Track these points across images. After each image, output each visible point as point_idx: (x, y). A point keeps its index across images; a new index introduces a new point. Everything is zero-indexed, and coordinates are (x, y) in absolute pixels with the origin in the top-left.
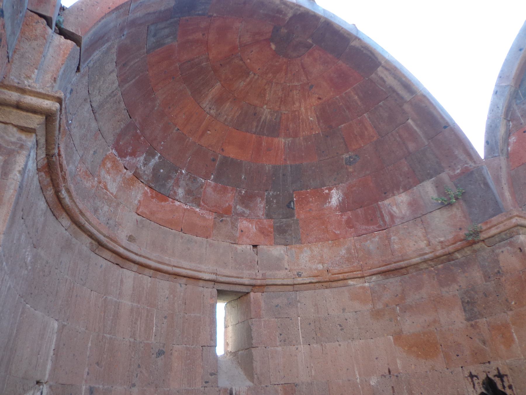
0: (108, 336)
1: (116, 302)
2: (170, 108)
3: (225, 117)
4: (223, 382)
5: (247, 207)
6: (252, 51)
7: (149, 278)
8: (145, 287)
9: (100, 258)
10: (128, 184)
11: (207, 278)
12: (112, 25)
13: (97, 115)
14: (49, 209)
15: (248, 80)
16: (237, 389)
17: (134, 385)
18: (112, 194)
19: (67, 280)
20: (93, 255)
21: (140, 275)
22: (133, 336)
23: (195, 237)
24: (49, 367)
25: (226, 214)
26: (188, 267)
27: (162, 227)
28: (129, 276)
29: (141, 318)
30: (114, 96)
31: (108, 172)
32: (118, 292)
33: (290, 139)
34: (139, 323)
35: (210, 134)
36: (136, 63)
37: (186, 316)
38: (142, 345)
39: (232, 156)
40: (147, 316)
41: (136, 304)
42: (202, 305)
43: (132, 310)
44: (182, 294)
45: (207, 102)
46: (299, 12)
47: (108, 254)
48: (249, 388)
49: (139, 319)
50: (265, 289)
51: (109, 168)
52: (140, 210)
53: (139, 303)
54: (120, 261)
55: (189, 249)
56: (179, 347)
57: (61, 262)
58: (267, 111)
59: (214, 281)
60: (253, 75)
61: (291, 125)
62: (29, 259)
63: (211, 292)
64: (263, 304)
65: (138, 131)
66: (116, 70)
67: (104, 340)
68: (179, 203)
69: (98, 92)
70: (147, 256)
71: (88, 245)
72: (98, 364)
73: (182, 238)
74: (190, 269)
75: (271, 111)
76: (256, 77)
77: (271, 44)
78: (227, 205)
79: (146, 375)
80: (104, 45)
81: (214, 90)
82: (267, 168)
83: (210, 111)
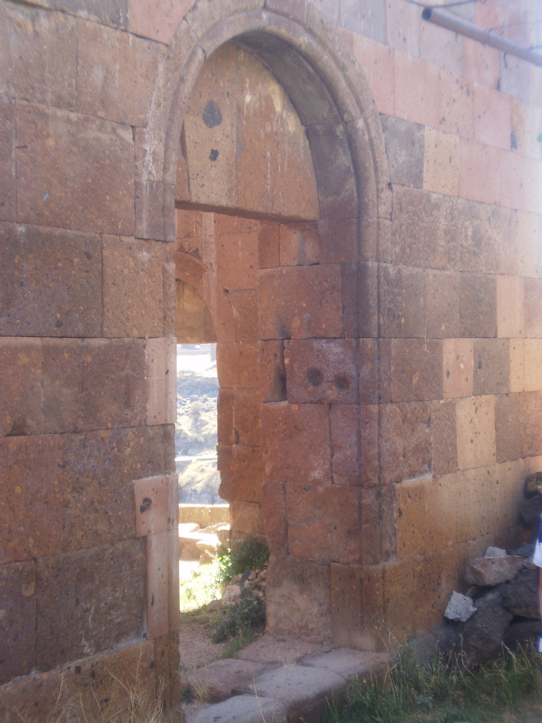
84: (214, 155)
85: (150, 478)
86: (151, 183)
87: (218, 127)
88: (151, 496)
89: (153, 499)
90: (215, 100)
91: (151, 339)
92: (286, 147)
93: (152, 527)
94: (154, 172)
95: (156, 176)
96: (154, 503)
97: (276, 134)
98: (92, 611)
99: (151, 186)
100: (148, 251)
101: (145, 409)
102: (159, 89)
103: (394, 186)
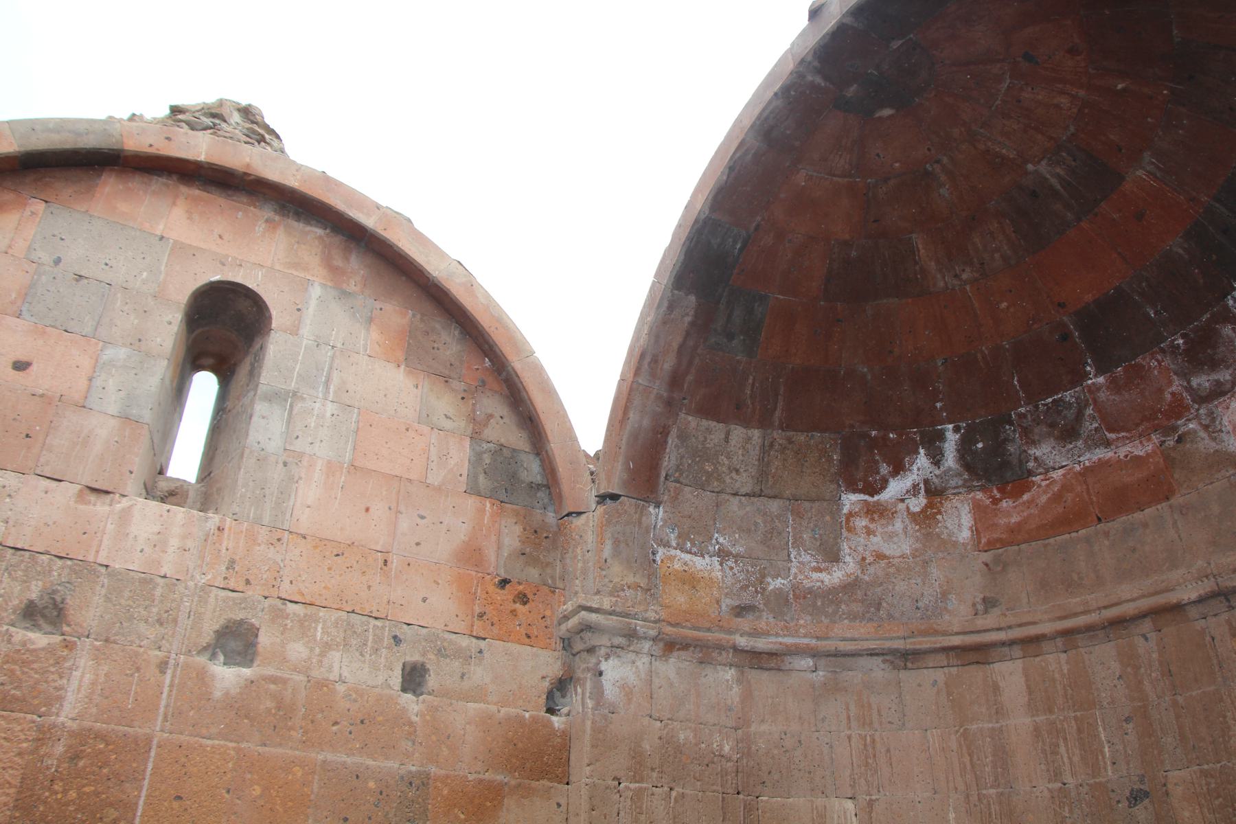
0: (992, 791)
1: (993, 729)
2: (891, 352)
3: (997, 256)
5: (1214, 365)
6: (878, 155)
7: (1063, 656)
8: (1057, 676)
9: (925, 671)
10: (926, 518)
12: (646, 422)
13: (766, 492)
14: (746, 669)
15: (943, 178)
18: (902, 556)
19: (849, 738)
20: (903, 675)
21: (1038, 659)
22: (1056, 775)
23: (1138, 516)
25: (1179, 417)
26: (1135, 595)
27: (1052, 540)
28: (1010, 675)
29: (1065, 739)
30: (771, 445)
31: (869, 532)
32: (993, 711)
33: (1147, 156)
34: (1062, 749)
35: (1008, 308)
36: (753, 384)
37: (1179, 698)
38: (1085, 789)
39: (1089, 298)
40: (1079, 731)
41: (1043, 718)
42: (1215, 662)
44: (1155, 656)
45: (939, 276)
46: (816, 63)
47: (941, 659)
49: (1061, 743)
51: (866, 527)
52: (984, 541)
53: (1051, 711)
54: (973, 656)
55: (1134, 550)
56: (1182, 773)
57: (823, 720)
58: (1043, 168)
60: (937, 168)
61: (1112, 137)
62: (727, 748)
63: (1229, 622)
65: (874, 433)
66: (733, 427)
67: (985, 801)
68: (1061, 472)
69: (734, 475)
70: (1024, 621)
71: (882, 666)
73: (1107, 534)
74: (1143, 596)
75: (1050, 159)
76: (945, 160)
77: (877, 115)
78: (1168, 397)
80: (666, 442)
81: (922, 251)
82: (1180, 251)
83: (961, 280)
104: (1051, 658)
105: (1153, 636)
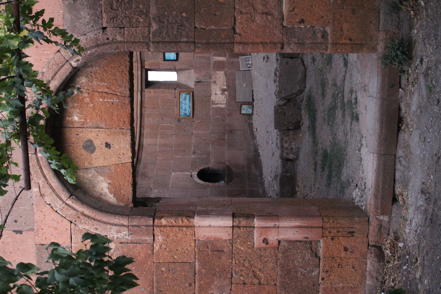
4: (191, 84)
11: (140, 97)
16: (195, 79)
17: (192, 133)
24: (186, 173)
34: (167, 133)
40: (163, 129)
41: (159, 136)
43: (161, 138)
47: (140, 154)
48: (195, 71)
50: (143, 60)
53: (157, 134)
54: (141, 148)
59: (142, 91)
63: (147, 93)
64: (152, 61)
72: (184, 152)
79: (188, 127)
84: (108, 145)
85: (255, 237)
86: (130, 234)
87: (94, 142)
88: (262, 239)
89: (264, 237)
90: (82, 144)
91: (196, 236)
92: (95, 83)
93: (276, 238)
94: (125, 233)
95: (126, 232)
96: (265, 237)
97: (89, 94)
98: (302, 270)
99: (131, 234)
100: (158, 236)
101: (225, 240)
102: (90, 228)
103: (104, 26)
104: (145, 132)
105: (146, 109)
